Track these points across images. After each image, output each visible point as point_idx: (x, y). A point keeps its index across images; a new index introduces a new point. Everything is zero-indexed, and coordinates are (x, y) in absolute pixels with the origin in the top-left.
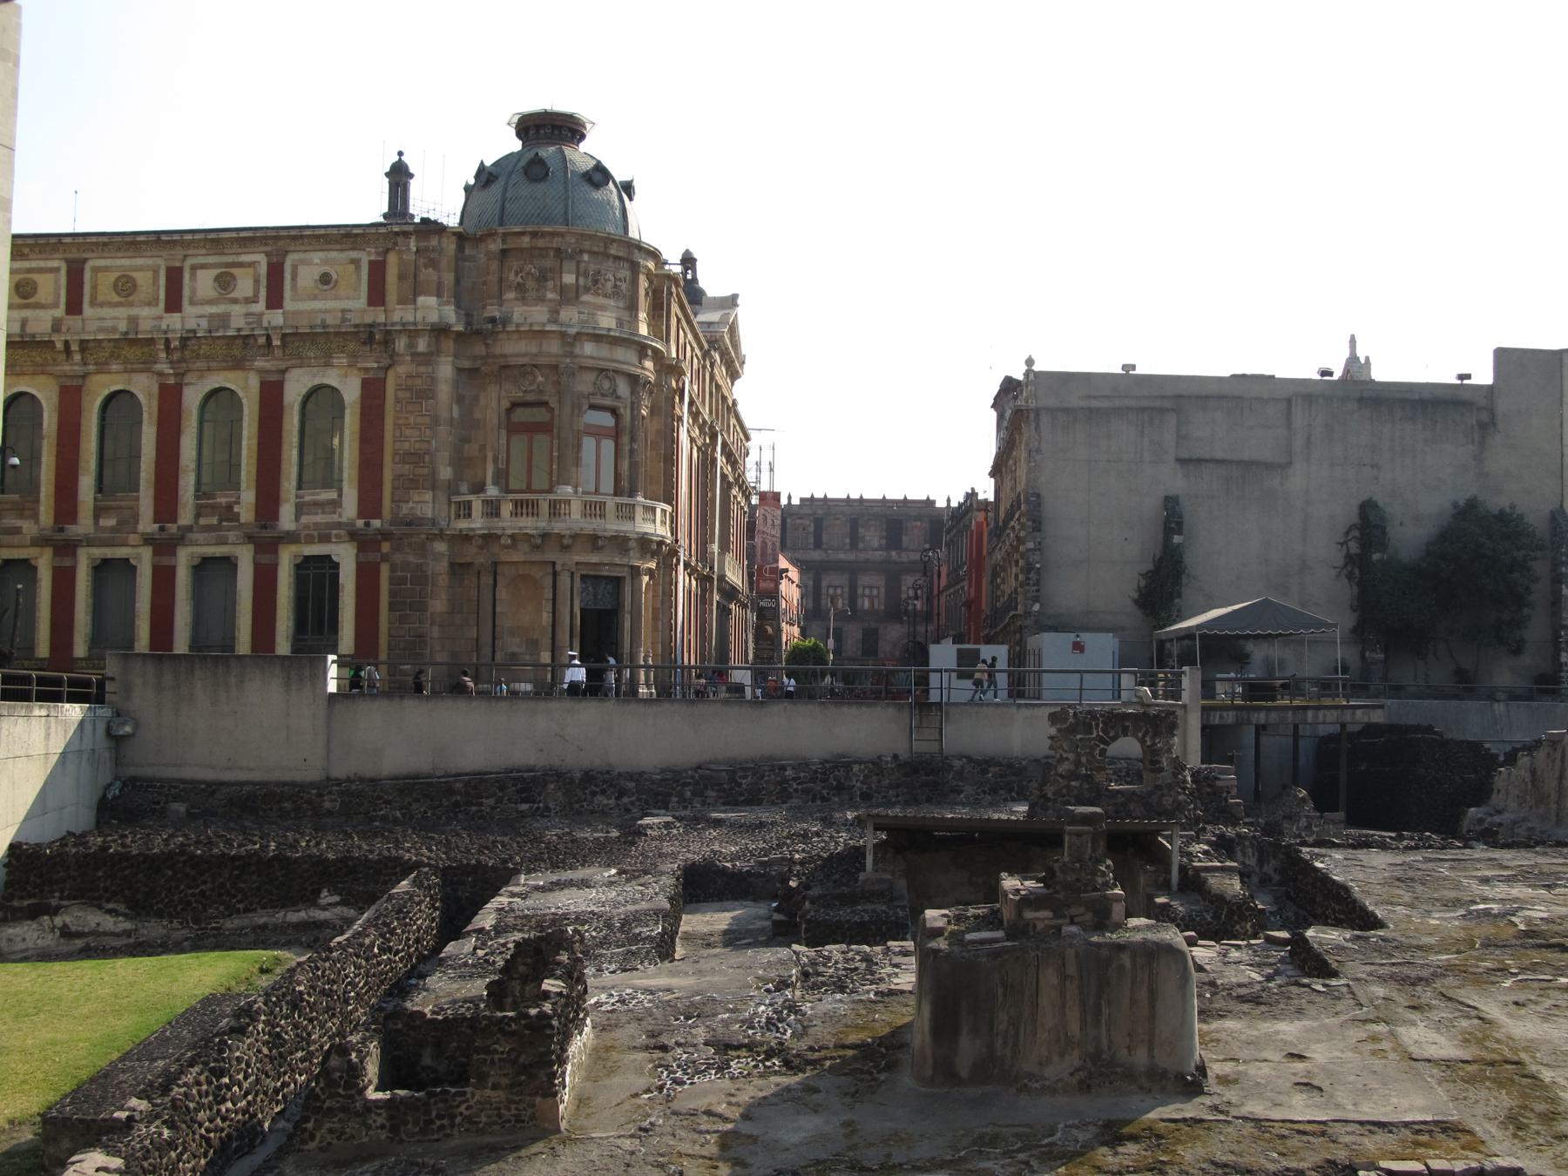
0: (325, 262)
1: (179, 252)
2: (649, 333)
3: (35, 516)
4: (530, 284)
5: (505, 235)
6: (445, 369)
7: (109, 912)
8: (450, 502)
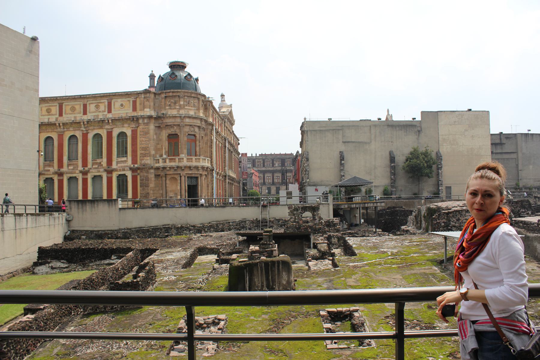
0: (122, 101)
1: (86, 100)
3: (53, 166)
4: (172, 105)
5: (166, 92)
6: (152, 127)
7: (62, 262)
8: (154, 159)
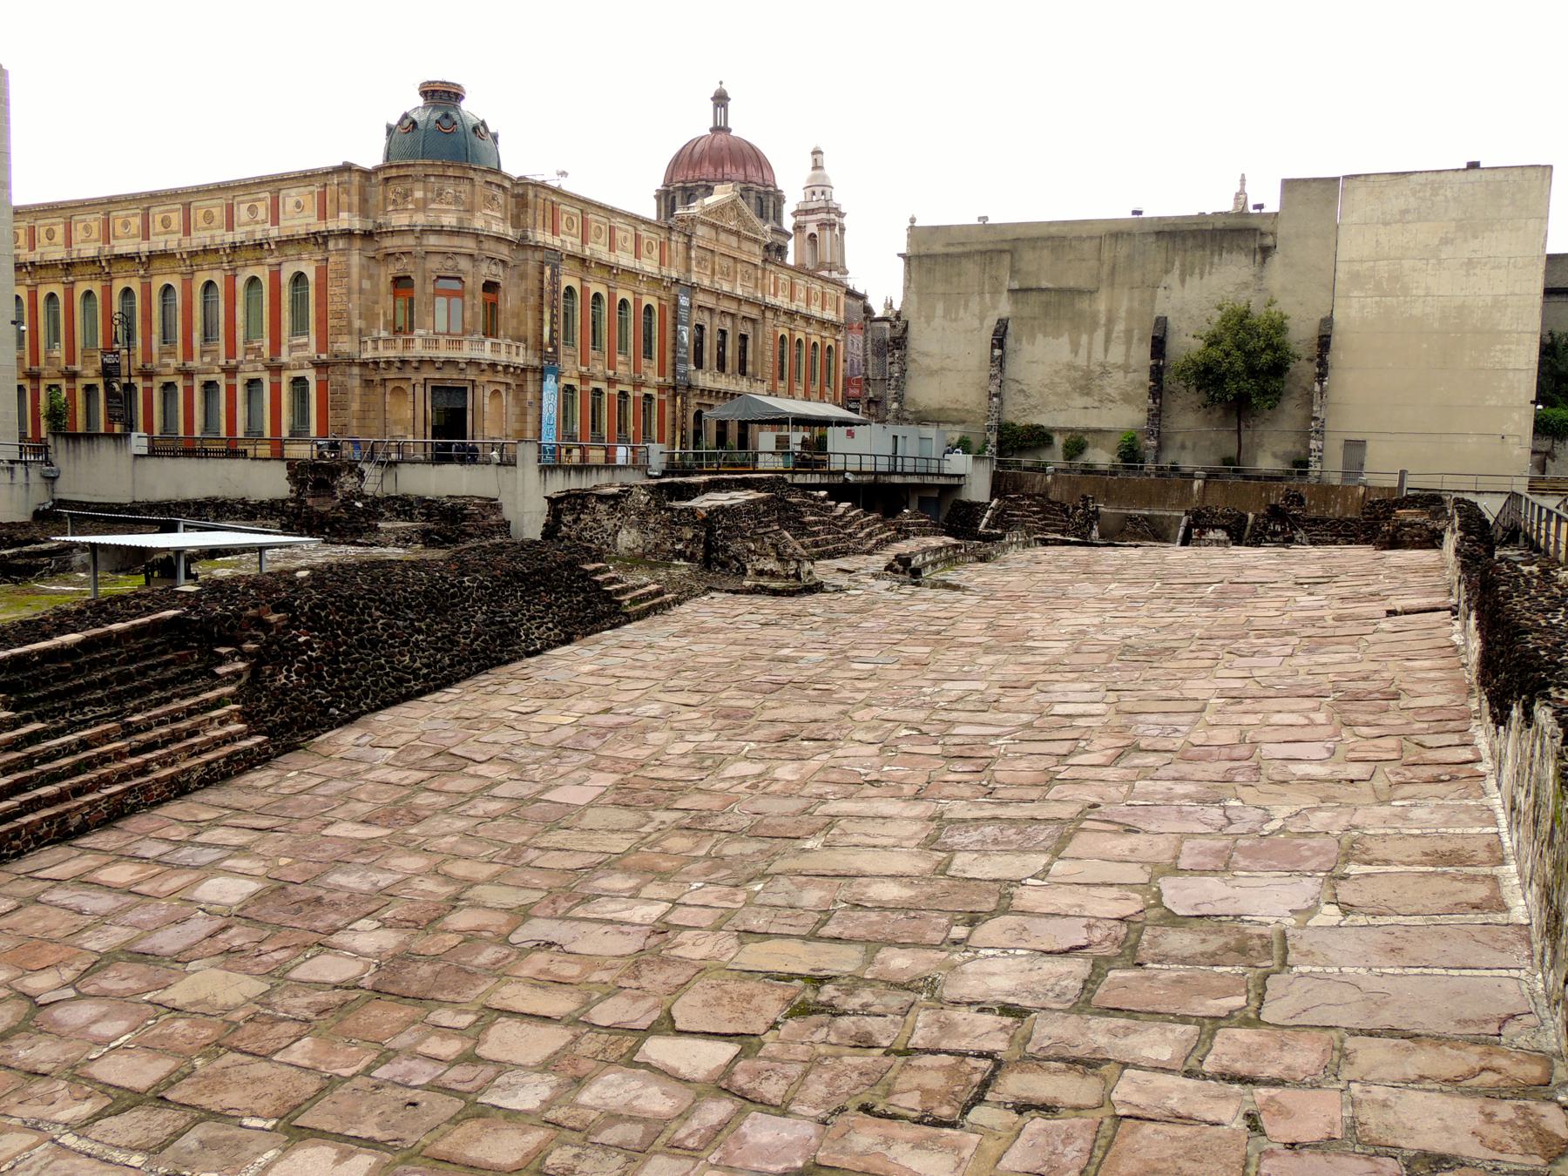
2: (659, 216)
4: (399, 201)
6: (355, 259)
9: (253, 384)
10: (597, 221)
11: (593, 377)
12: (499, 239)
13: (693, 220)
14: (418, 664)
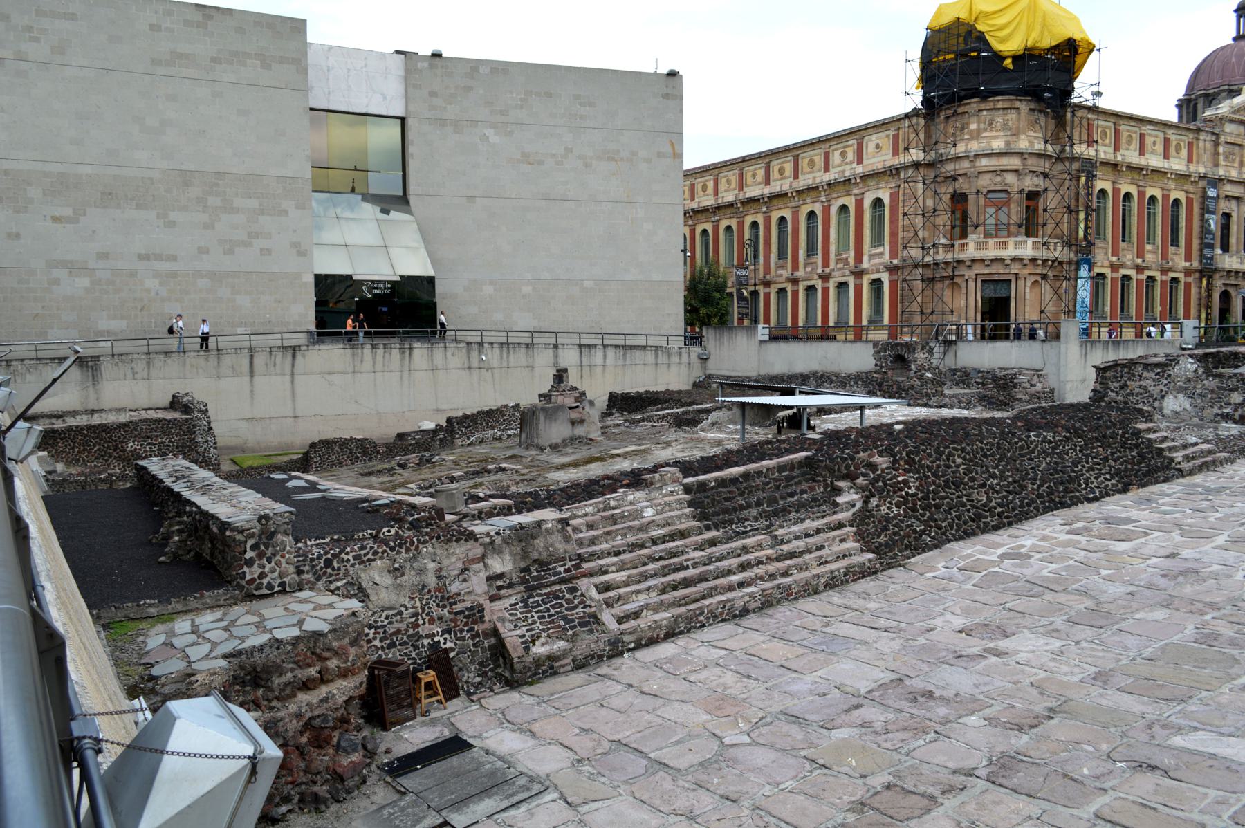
0: (878, 139)
1: (827, 145)
9: (842, 286)
10: (1128, 131)
11: (1123, 266)
12: (1041, 155)
13: (1222, 119)
14: (993, 504)
